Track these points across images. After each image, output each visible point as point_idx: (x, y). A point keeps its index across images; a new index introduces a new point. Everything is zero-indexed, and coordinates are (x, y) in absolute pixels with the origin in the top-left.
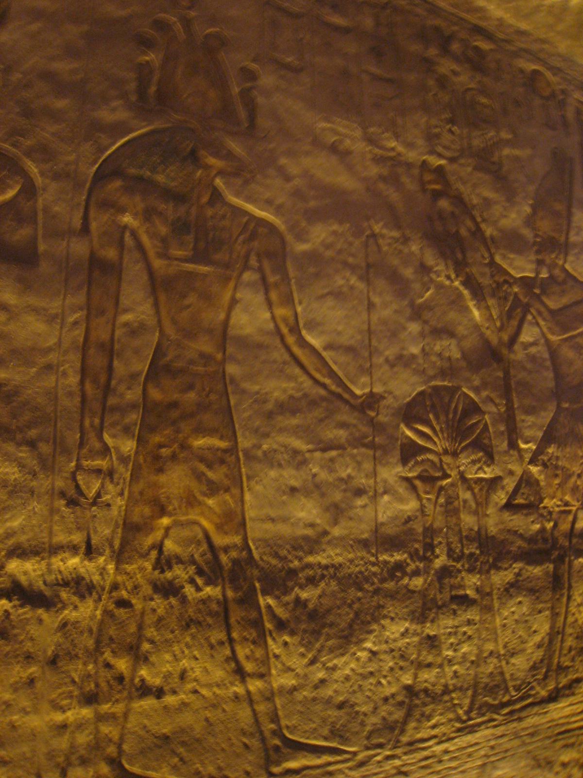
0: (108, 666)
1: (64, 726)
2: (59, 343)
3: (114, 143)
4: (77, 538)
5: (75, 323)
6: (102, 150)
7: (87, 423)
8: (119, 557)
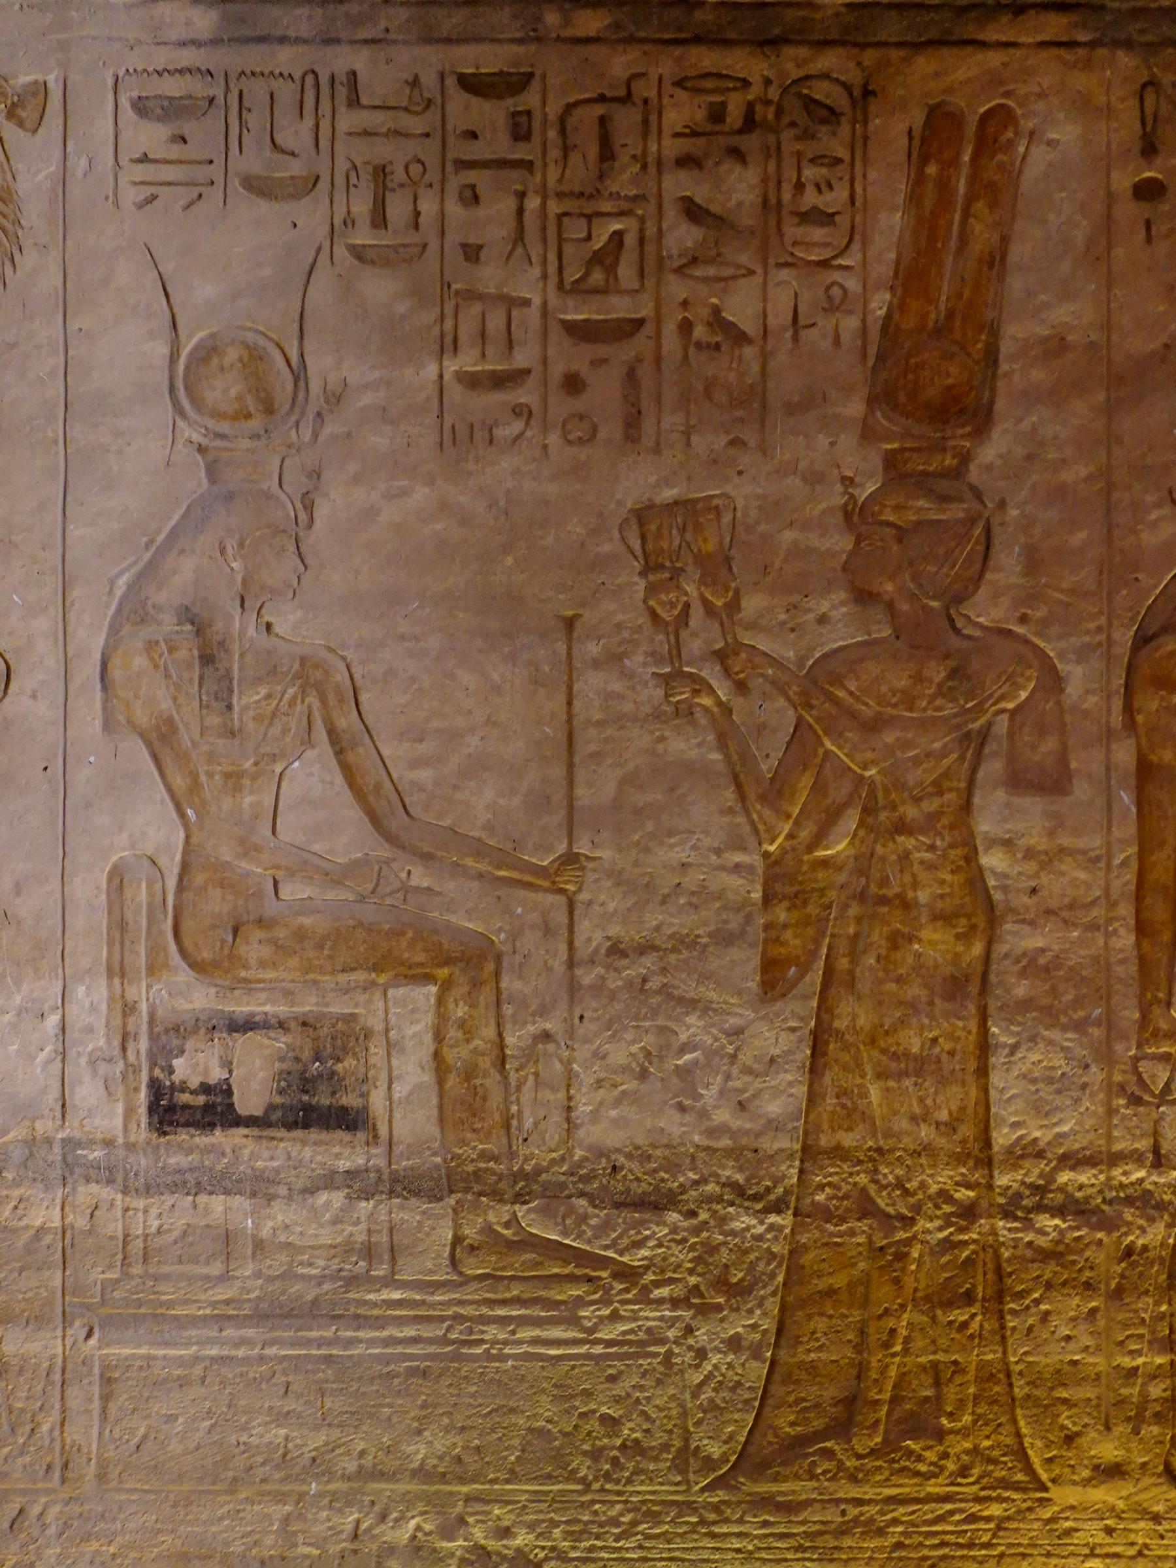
4: (1143, 1144)
5: (1124, 864)
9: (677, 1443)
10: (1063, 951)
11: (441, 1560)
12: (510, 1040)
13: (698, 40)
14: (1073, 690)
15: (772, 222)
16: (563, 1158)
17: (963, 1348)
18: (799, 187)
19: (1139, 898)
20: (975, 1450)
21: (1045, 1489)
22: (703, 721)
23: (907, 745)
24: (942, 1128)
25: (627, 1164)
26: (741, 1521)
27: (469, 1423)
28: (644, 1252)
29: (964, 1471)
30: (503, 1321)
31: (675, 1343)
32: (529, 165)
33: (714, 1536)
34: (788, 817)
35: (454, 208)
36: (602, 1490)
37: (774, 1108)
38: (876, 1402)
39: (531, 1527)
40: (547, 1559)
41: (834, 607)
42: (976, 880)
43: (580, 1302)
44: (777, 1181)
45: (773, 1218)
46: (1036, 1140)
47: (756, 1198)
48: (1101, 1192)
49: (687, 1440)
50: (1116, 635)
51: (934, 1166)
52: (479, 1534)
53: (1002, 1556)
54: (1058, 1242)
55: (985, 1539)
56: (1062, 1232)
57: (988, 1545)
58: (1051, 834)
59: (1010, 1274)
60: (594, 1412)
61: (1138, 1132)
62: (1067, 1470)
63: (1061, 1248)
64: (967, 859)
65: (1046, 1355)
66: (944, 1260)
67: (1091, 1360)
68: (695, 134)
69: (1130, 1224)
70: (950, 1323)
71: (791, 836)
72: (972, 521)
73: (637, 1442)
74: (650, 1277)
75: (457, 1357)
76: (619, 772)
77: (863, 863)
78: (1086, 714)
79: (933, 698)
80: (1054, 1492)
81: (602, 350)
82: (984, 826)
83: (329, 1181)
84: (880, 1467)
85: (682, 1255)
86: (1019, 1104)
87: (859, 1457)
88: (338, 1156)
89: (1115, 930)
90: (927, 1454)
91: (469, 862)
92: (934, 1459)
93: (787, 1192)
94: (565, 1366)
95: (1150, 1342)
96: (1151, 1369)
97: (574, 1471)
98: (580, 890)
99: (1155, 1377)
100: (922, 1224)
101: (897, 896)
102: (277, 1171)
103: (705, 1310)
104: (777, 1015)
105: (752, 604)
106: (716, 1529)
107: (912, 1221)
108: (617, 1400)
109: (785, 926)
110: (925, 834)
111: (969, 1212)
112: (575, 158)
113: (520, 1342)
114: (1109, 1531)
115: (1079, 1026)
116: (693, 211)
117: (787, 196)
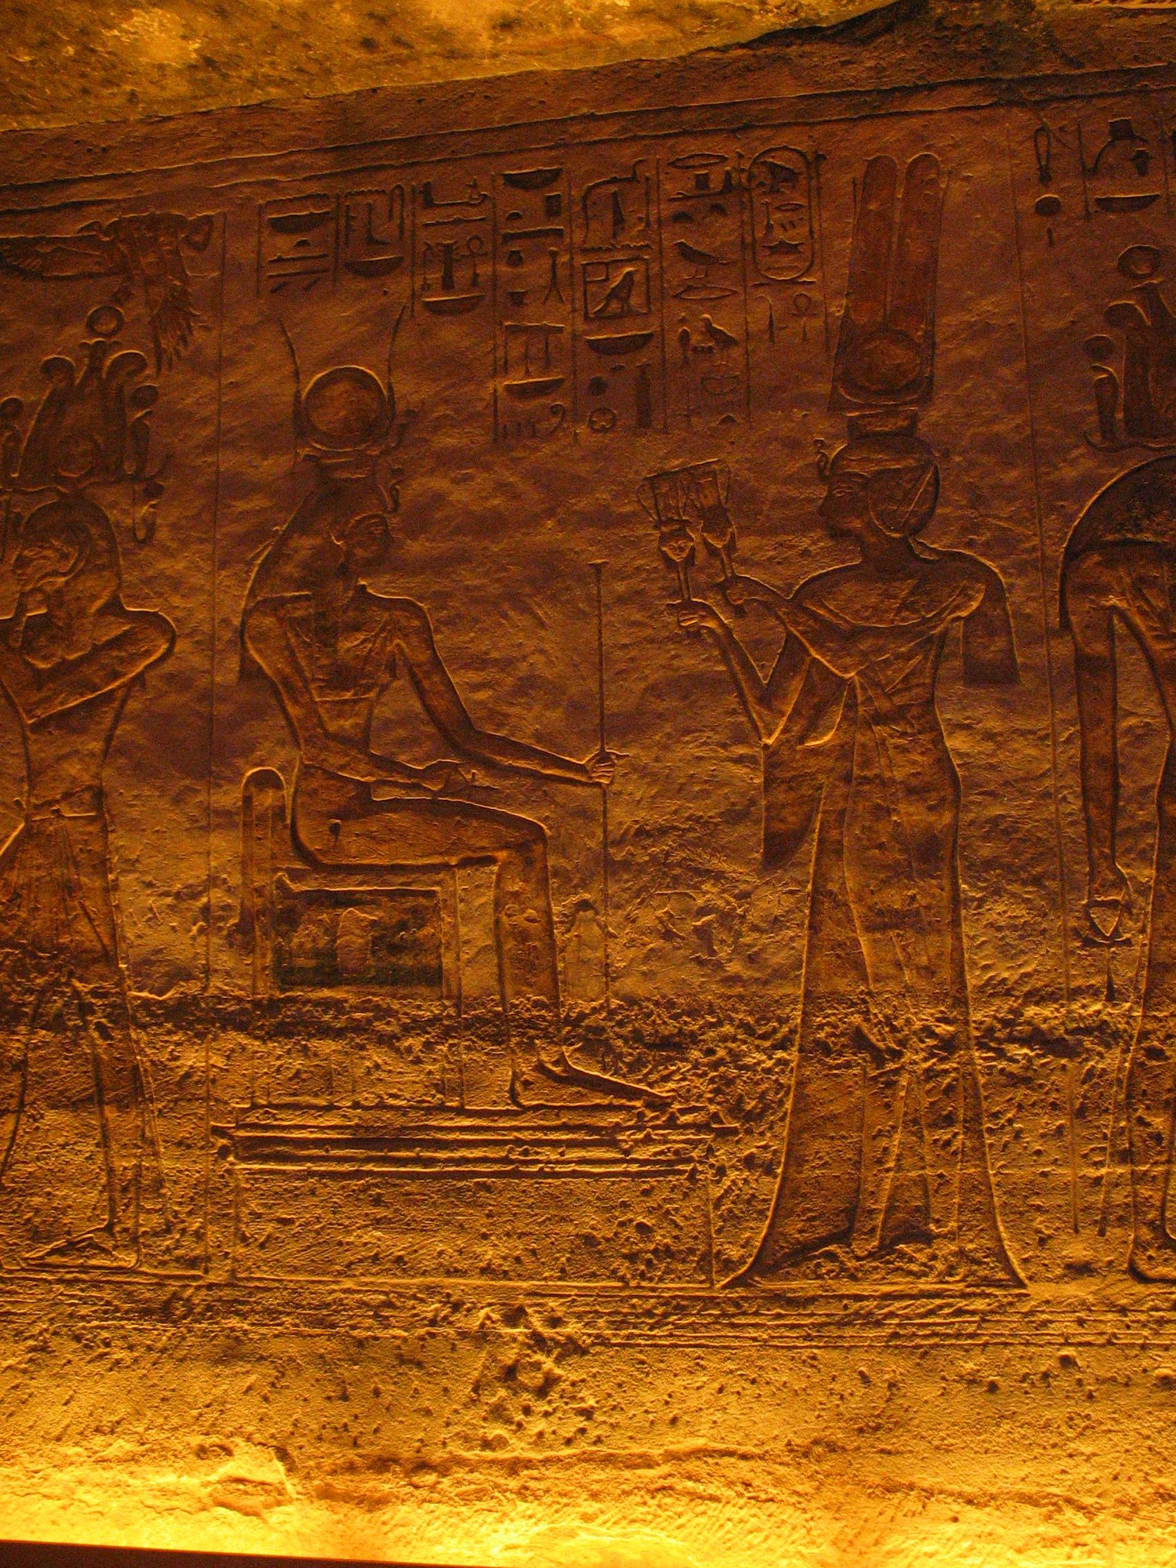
0: (1141, 1121)
1: (1097, 1181)
2: (1055, 764)
3: (1082, 507)
5: (1069, 740)
6: (1072, 517)
7: (1096, 852)
8: (1148, 1000)
9: (702, 1247)
10: (1020, 817)
11: (505, 1343)
12: (556, 909)
13: (685, 133)
14: (1014, 598)
15: (749, 257)
16: (602, 1007)
17: (947, 1163)
18: (769, 228)
19: (1083, 769)
20: (961, 1253)
21: (1023, 1286)
22: (710, 641)
23: (880, 651)
24: (923, 972)
25: (656, 1010)
26: (756, 1314)
27: (527, 1229)
28: (671, 1085)
29: (951, 1271)
30: (555, 1144)
31: (701, 1162)
32: (559, 233)
33: (733, 1326)
34: (782, 714)
35: (503, 269)
36: (639, 1287)
37: (779, 959)
38: (871, 1212)
39: (579, 1316)
40: (593, 1344)
41: (814, 543)
42: (943, 761)
43: (618, 1128)
44: (782, 1021)
45: (780, 1054)
46: (1005, 980)
47: (764, 1037)
48: (1063, 1023)
49: (710, 1246)
50: (1049, 553)
51: (916, 1006)
52: (537, 1323)
53: (986, 1345)
54: (1027, 1068)
55: (971, 1329)
56: (1030, 1060)
57: (971, 1336)
58: (1004, 718)
59: (986, 1098)
60: (631, 1220)
61: (1092, 970)
62: (1042, 1268)
63: (1030, 1074)
64: (934, 742)
65: (1020, 1168)
66: (928, 1087)
67: (1060, 1171)
68: (687, 198)
69: (1088, 1051)
70: (936, 1141)
71: (785, 731)
72: (924, 469)
73: (667, 1246)
74: (676, 1106)
75: (516, 1174)
76: (642, 685)
77: (843, 751)
78: (1028, 616)
79: (899, 611)
80: (1032, 1289)
81: (621, 361)
82: (945, 715)
83: (415, 1026)
84: (876, 1268)
85: (702, 1086)
86: (989, 949)
87: (858, 1258)
88: (419, 1007)
89: (1064, 798)
90: (917, 1255)
91: (522, 764)
92: (924, 1260)
93: (793, 1031)
94: (607, 1182)
95: (1112, 1155)
96: (1114, 1178)
97: (614, 1272)
98: (612, 783)
99: (1117, 1185)
100: (909, 1056)
101: (877, 776)
102: (369, 1021)
103: (724, 1133)
104: (779, 881)
105: (746, 544)
106: (735, 1321)
107: (896, 1055)
108: (651, 1211)
109: (784, 806)
110: (897, 723)
111: (949, 1046)
112: (594, 225)
113: (570, 1162)
114: (1081, 1322)
115: (1037, 881)
116: (686, 253)
117: (759, 235)
